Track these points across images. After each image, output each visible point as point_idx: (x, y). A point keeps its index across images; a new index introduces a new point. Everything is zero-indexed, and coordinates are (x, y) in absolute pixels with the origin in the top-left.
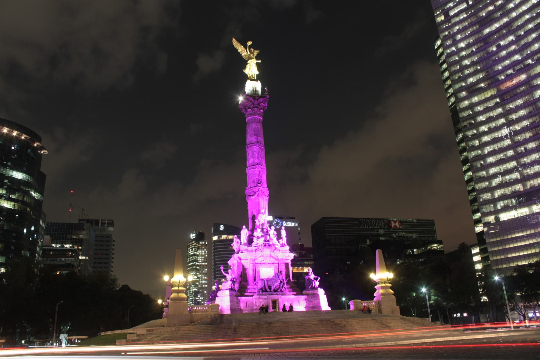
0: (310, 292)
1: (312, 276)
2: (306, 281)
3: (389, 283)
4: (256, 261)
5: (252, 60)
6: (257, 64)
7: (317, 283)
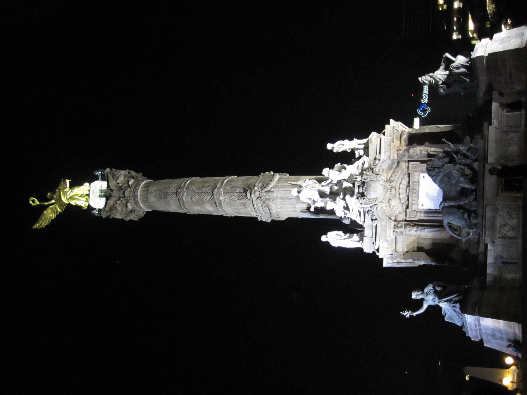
0: (483, 80)
1: (441, 74)
2: (451, 90)
4: (401, 217)
6: (72, 186)
7: (461, 60)
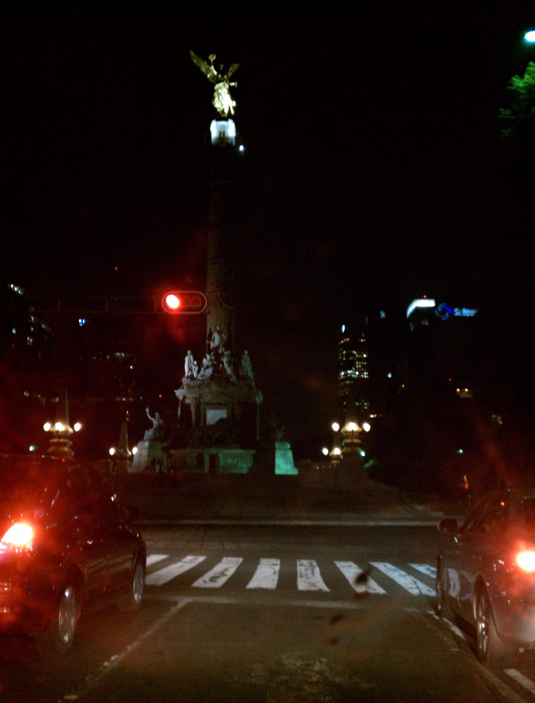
3: (359, 439)
4: (201, 400)
5: (221, 84)
